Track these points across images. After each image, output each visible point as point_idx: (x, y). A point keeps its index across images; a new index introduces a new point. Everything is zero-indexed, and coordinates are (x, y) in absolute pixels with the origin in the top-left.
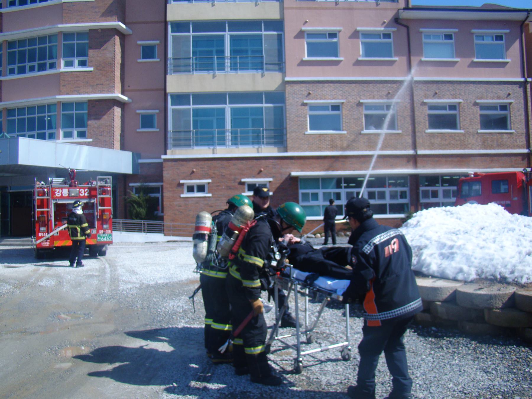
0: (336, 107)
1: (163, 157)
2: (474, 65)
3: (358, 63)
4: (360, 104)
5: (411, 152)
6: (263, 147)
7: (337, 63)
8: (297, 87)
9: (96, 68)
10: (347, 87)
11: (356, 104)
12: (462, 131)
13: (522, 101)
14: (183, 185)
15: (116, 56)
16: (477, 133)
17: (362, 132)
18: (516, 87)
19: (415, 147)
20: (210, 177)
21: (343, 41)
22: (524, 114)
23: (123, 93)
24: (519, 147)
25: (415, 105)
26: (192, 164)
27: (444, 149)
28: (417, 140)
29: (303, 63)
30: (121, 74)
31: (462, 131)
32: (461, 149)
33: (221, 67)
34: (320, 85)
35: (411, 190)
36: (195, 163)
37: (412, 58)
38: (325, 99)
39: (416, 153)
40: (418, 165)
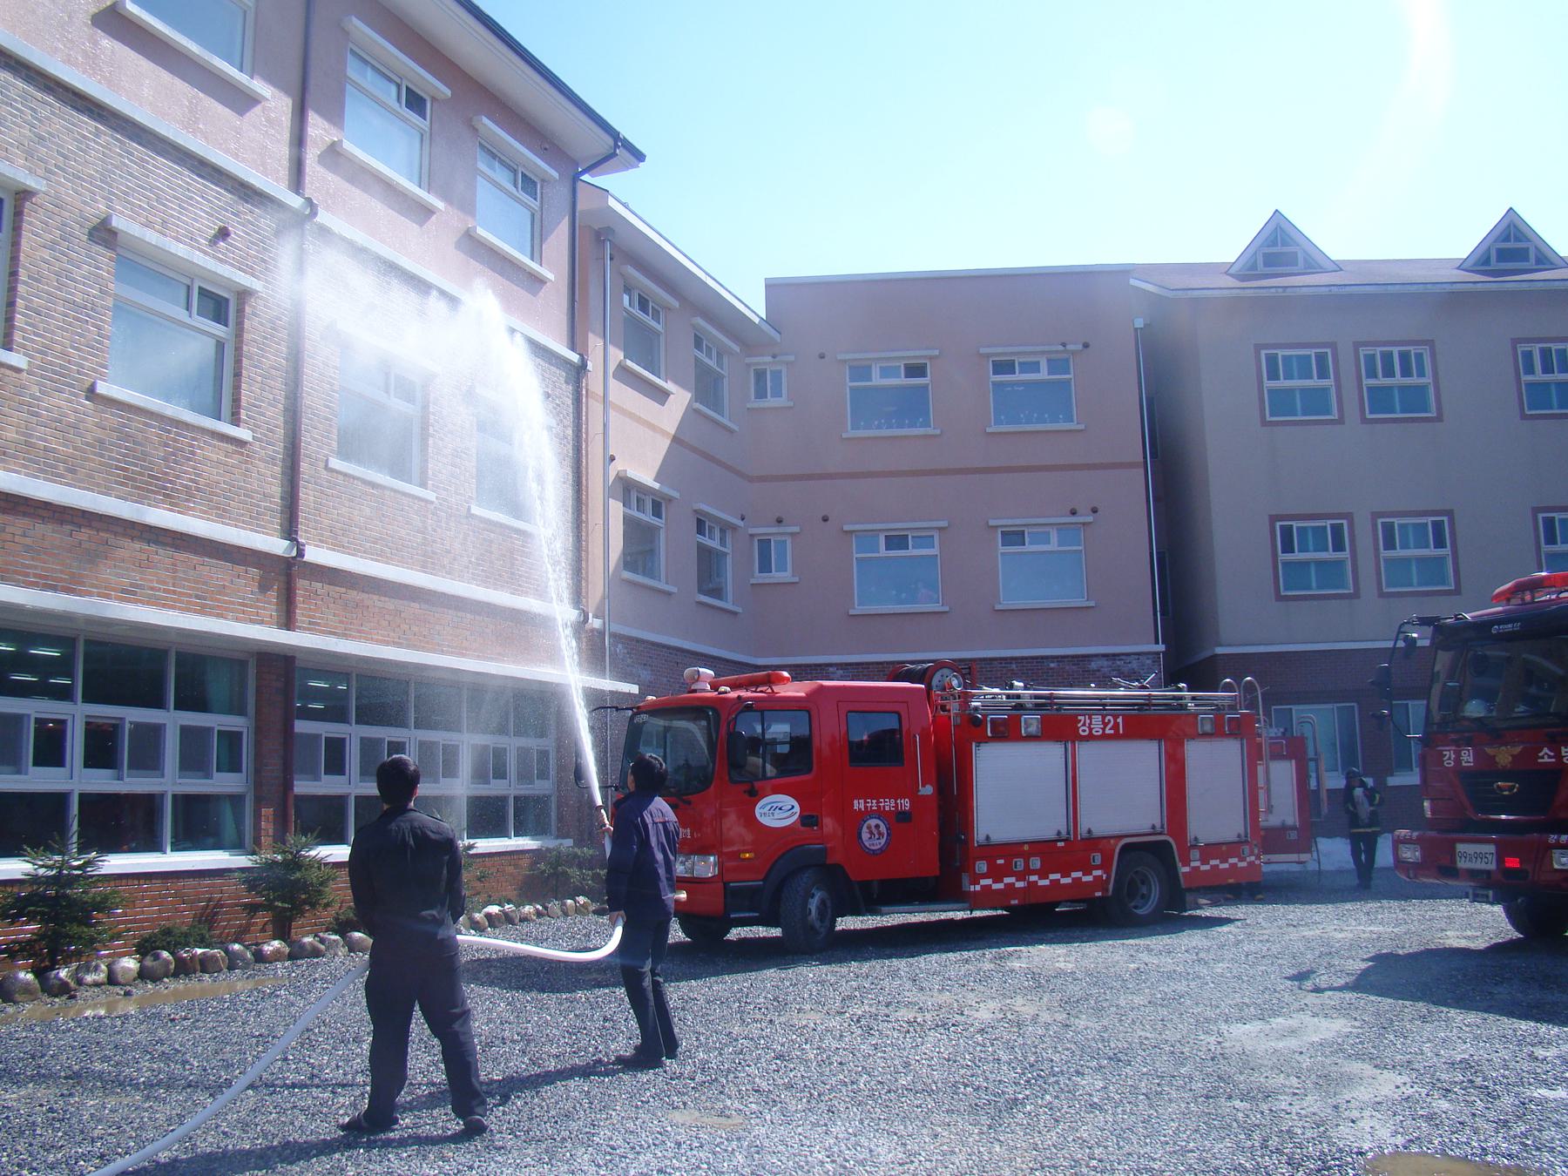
4: (104, 233)
5: (277, 545)
11: (89, 225)
16: (470, 515)
17: (102, 388)
35: (259, 730)
39: (301, 553)
40: (300, 615)
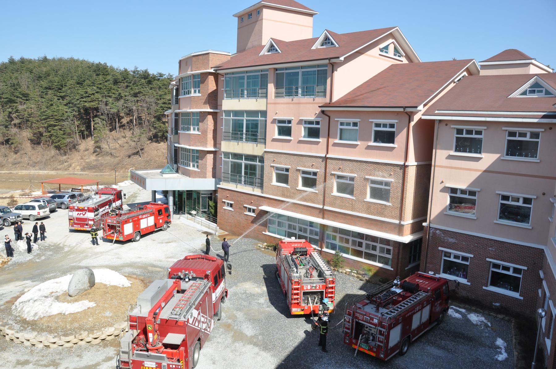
0: (287, 170)
1: (218, 186)
2: (369, 148)
3: (300, 142)
6: (256, 187)
7: (289, 141)
8: (269, 155)
9: (202, 133)
10: (292, 157)
12: (354, 198)
13: (401, 181)
14: (225, 202)
15: (209, 127)
16: (364, 201)
18: (398, 169)
19: (324, 205)
20: (234, 201)
21: (293, 125)
22: (400, 191)
23: (215, 145)
24: (393, 218)
25: (327, 175)
26: (228, 192)
27: (342, 209)
28: (326, 199)
29: (274, 140)
30: (213, 136)
31: (354, 198)
32: (352, 210)
33: (241, 139)
34: (280, 155)
36: (229, 191)
37: (330, 139)
38: (281, 164)
40: (325, 216)
